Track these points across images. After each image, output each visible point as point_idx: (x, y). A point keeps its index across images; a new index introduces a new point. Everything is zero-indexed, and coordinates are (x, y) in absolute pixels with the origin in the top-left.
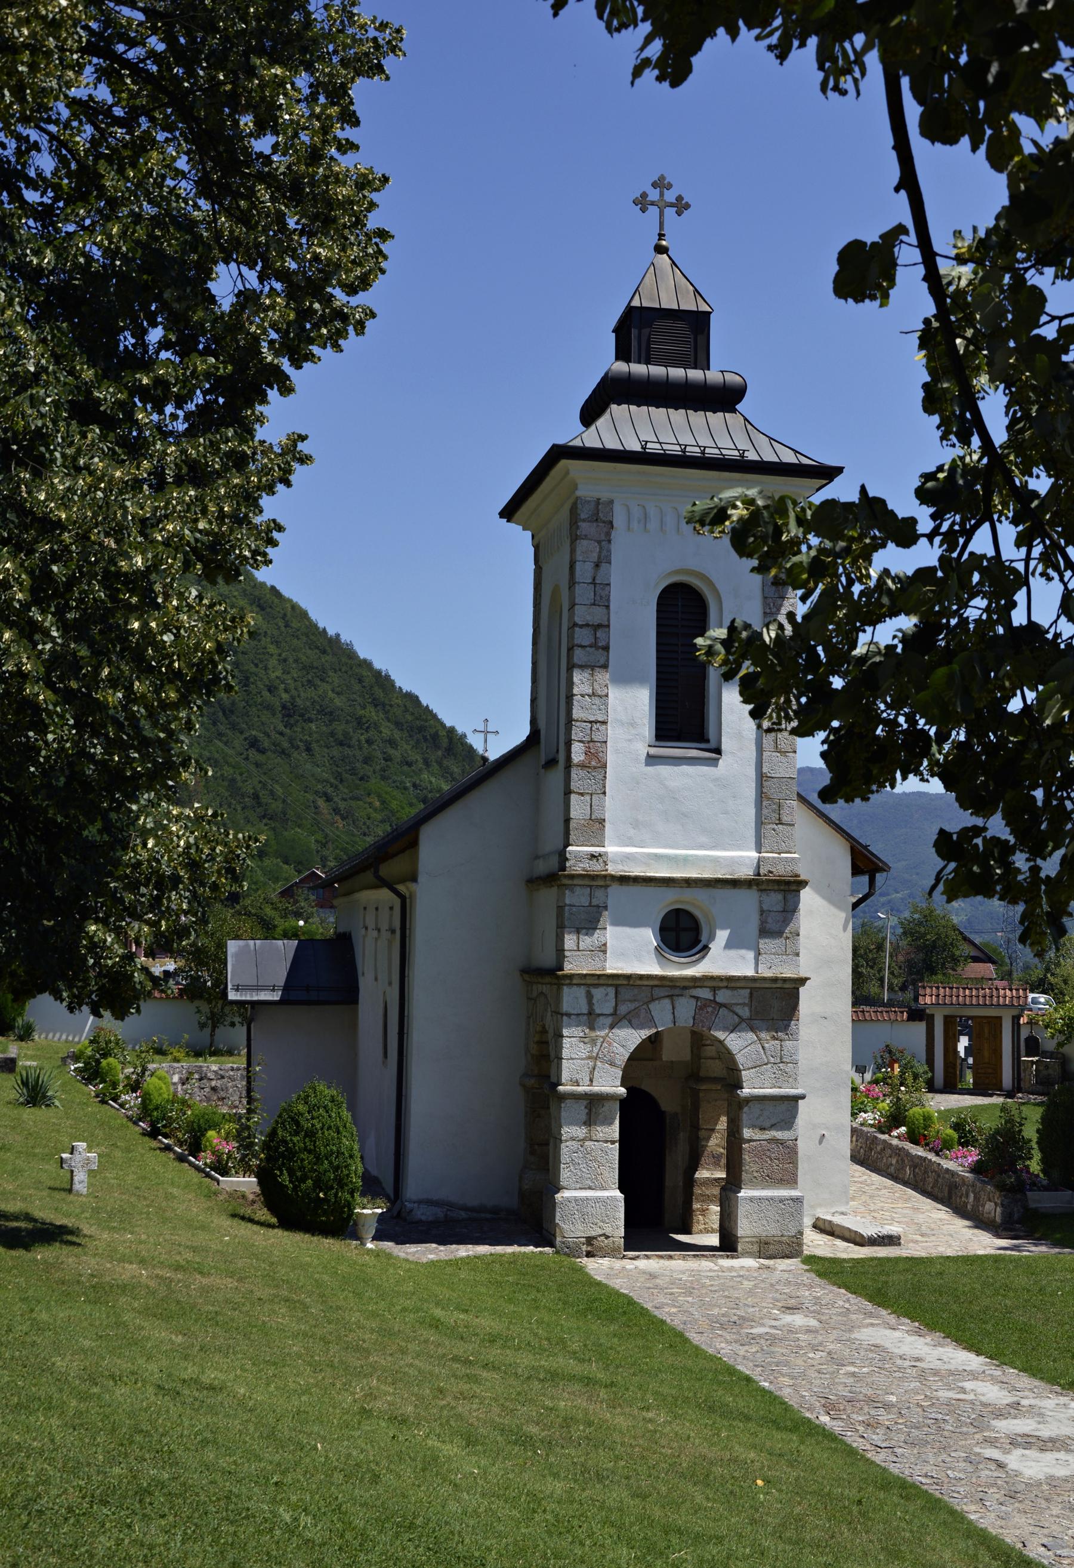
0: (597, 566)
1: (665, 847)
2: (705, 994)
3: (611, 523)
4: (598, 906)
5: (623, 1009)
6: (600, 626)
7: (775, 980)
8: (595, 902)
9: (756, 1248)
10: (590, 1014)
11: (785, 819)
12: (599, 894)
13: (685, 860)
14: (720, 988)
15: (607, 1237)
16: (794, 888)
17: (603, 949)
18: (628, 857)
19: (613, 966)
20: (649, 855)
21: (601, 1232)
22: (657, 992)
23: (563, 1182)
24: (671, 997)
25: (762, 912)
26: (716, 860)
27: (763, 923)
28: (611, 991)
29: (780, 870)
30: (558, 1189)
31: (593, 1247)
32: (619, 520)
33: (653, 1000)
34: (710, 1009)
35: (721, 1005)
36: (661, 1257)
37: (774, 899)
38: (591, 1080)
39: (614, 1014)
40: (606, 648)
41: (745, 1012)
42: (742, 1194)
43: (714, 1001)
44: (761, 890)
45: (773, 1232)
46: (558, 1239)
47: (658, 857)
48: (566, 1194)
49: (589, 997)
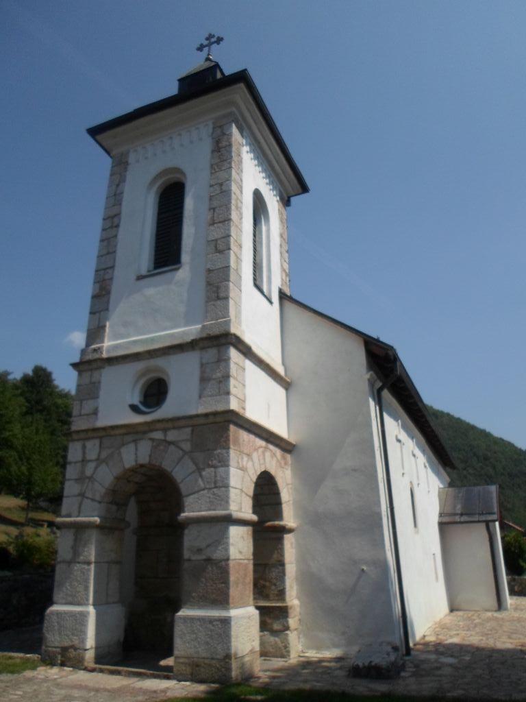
0: (118, 185)
1: (145, 334)
2: (158, 435)
3: (127, 162)
4: (94, 383)
5: (104, 454)
6: (115, 215)
7: (206, 415)
8: (93, 380)
9: (189, 670)
10: (83, 461)
11: (222, 295)
12: (96, 374)
13: (152, 340)
14: (169, 429)
15: (76, 649)
16: (223, 341)
17: (95, 413)
18: (116, 347)
19: (102, 422)
20: (129, 342)
21: (71, 644)
22: (129, 438)
23: (55, 598)
24: (135, 441)
25: (202, 365)
26: (172, 335)
27: (203, 372)
28: (97, 442)
29: (216, 331)
30: (50, 602)
31: (68, 658)
32: (132, 158)
33: (123, 445)
34: (162, 447)
35: (170, 443)
36: (112, 673)
37: (211, 354)
38: (79, 512)
39: (97, 459)
40: (118, 226)
41: (187, 446)
42: (183, 612)
43: (165, 441)
44: (203, 349)
45: (204, 655)
46: (44, 647)
47: (135, 342)
48: (55, 608)
49: (84, 447)
